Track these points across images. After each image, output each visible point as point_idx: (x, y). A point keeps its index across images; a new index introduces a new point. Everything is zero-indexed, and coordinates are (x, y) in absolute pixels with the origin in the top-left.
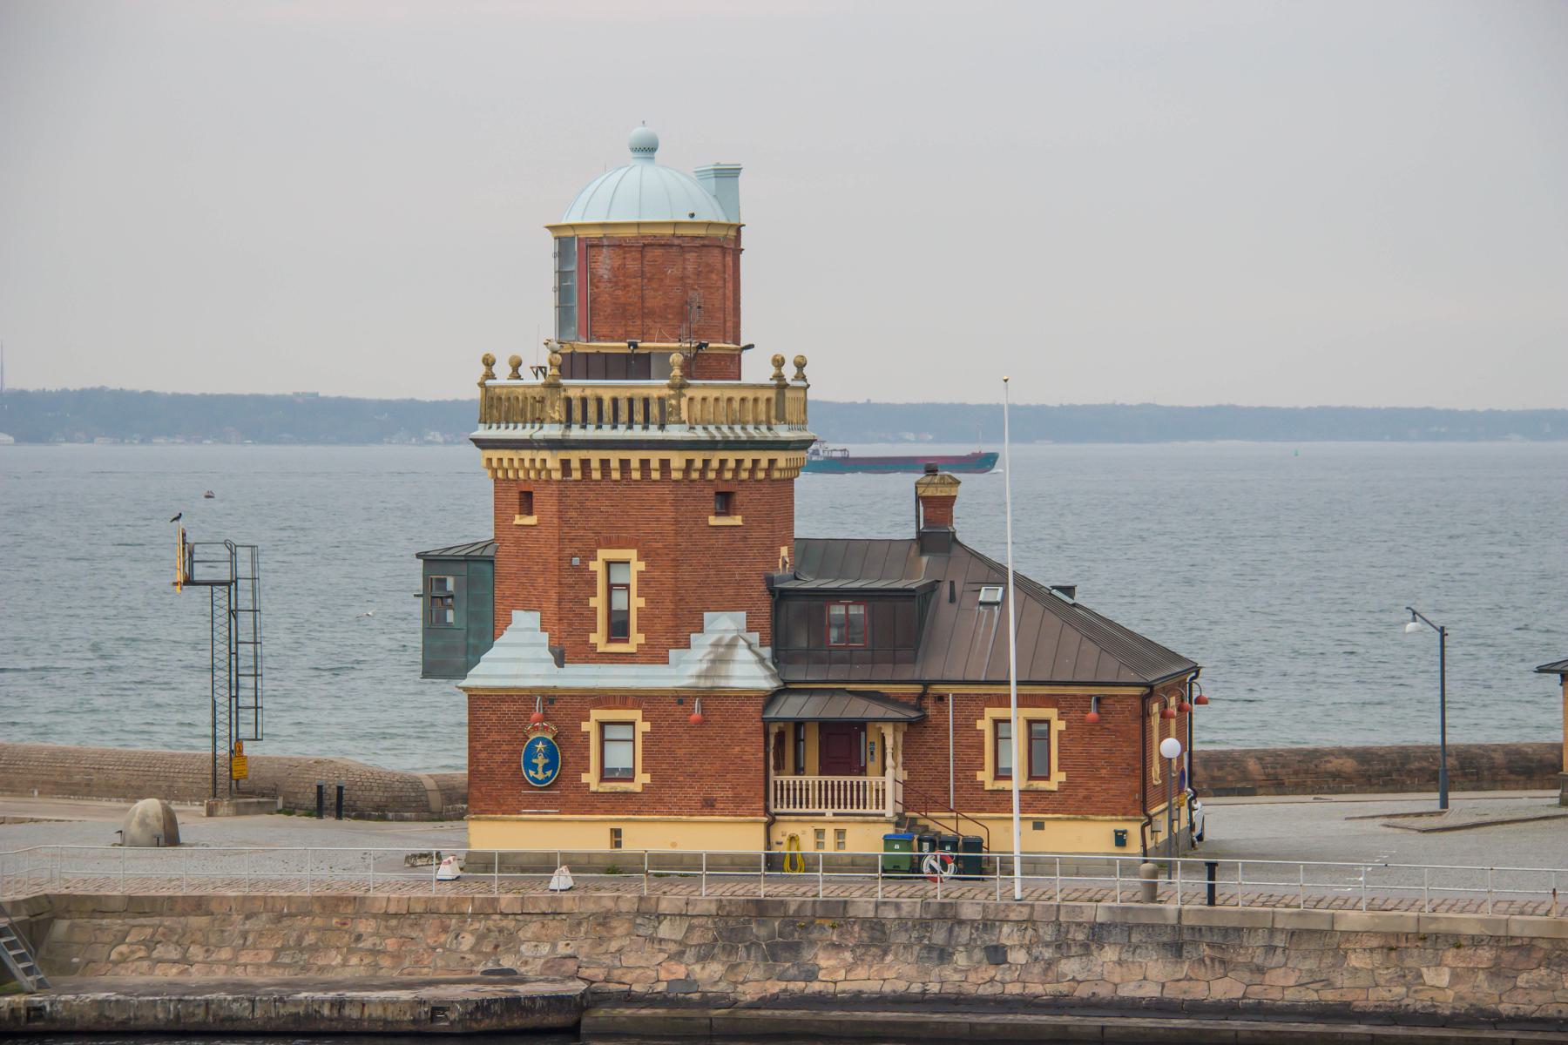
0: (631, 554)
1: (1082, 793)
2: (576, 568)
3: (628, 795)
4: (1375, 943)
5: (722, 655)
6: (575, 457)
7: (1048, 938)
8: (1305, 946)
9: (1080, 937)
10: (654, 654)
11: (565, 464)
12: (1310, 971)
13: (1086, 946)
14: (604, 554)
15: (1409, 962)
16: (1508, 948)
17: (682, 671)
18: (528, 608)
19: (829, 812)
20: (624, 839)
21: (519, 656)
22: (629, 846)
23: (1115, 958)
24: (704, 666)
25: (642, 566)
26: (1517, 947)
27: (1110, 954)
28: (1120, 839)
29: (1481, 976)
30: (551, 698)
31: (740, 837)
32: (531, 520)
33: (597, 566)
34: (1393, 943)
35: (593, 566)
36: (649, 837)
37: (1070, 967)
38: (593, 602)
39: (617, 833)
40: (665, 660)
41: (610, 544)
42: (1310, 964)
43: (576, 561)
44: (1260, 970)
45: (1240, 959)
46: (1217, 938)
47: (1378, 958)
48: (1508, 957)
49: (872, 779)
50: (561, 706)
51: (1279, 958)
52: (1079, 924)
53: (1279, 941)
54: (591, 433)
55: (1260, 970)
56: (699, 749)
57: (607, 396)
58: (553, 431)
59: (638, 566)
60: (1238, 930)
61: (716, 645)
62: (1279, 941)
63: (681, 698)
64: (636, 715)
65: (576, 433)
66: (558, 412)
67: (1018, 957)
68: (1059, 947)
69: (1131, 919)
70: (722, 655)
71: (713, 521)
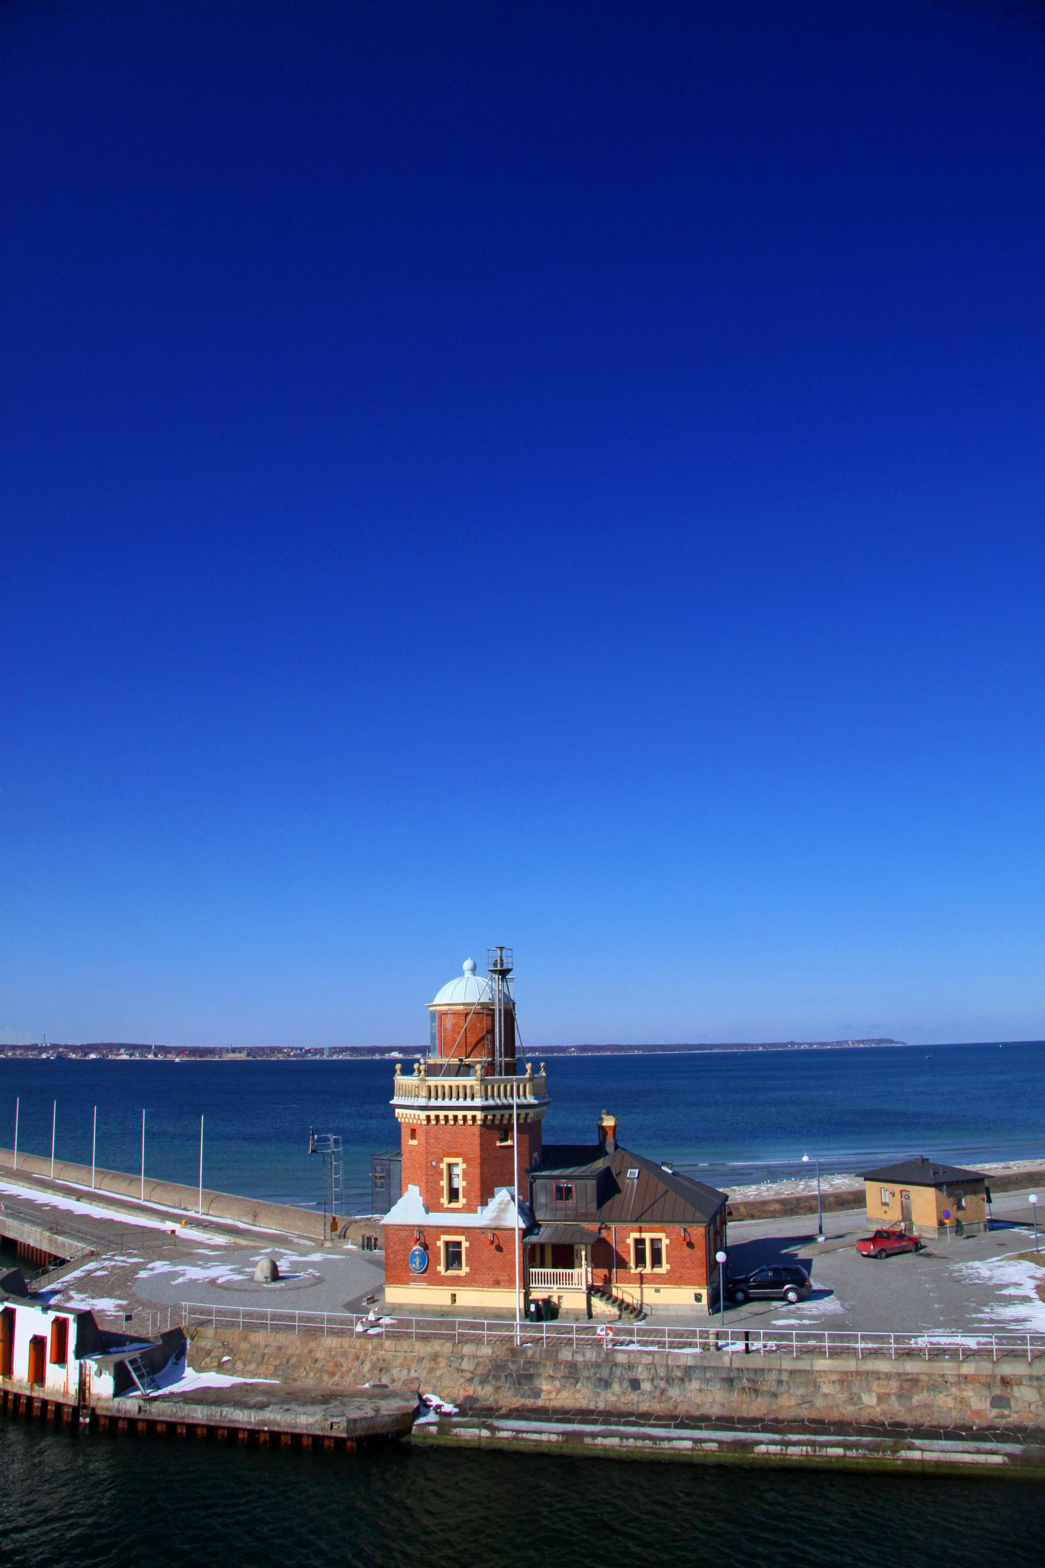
0: (459, 1160)
1: (678, 1275)
2: (435, 1167)
3: (458, 1277)
4: (835, 1377)
5: (502, 1210)
6: (432, 1114)
7: (662, 1375)
8: (798, 1380)
9: (679, 1374)
10: (469, 1209)
11: (428, 1118)
12: (802, 1396)
13: (682, 1380)
14: (448, 1160)
15: (855, 1390)
16: (906, 1380)
17: (482, 1218)
19: (555, 1286)
20: (457, 1298)
22: (459, 1302)
23: (698, 1387)
24: (495, 1214)
25: (464, 1166)
26: (910, 1380)
27: (695, 1385)
28: (698, 1298)
29: (893, 1398)
30: (421, 1229)
32: (415, 1142)
34: (844, 1377)
37: (674, 1392)
39: (454, 1296)
40: (475, 1212)
41: (449, 1155)
42: (801, 1391)
44: (775, 1395)
45: (765, 1388)
46: (751, 1375)
47: (837, 1386)
48: (906, 1385)
49: (575, 1271)
51: (785, 1387)
52: (678, 1367)
53: (785, 1377)
54: (440, 1102)
55: (775, 1395)
58: (422, 1102)
60: (763, 1370)
61: (501, 1203)
62: (785, 1377)
63: (482, 1229)
65: (433, 1102)
66: (424, 1092)
67: (646, 1386)
68: (668, 1381)
69: (706, 1364)
70: (502, 1210)
71: (498, 1144)
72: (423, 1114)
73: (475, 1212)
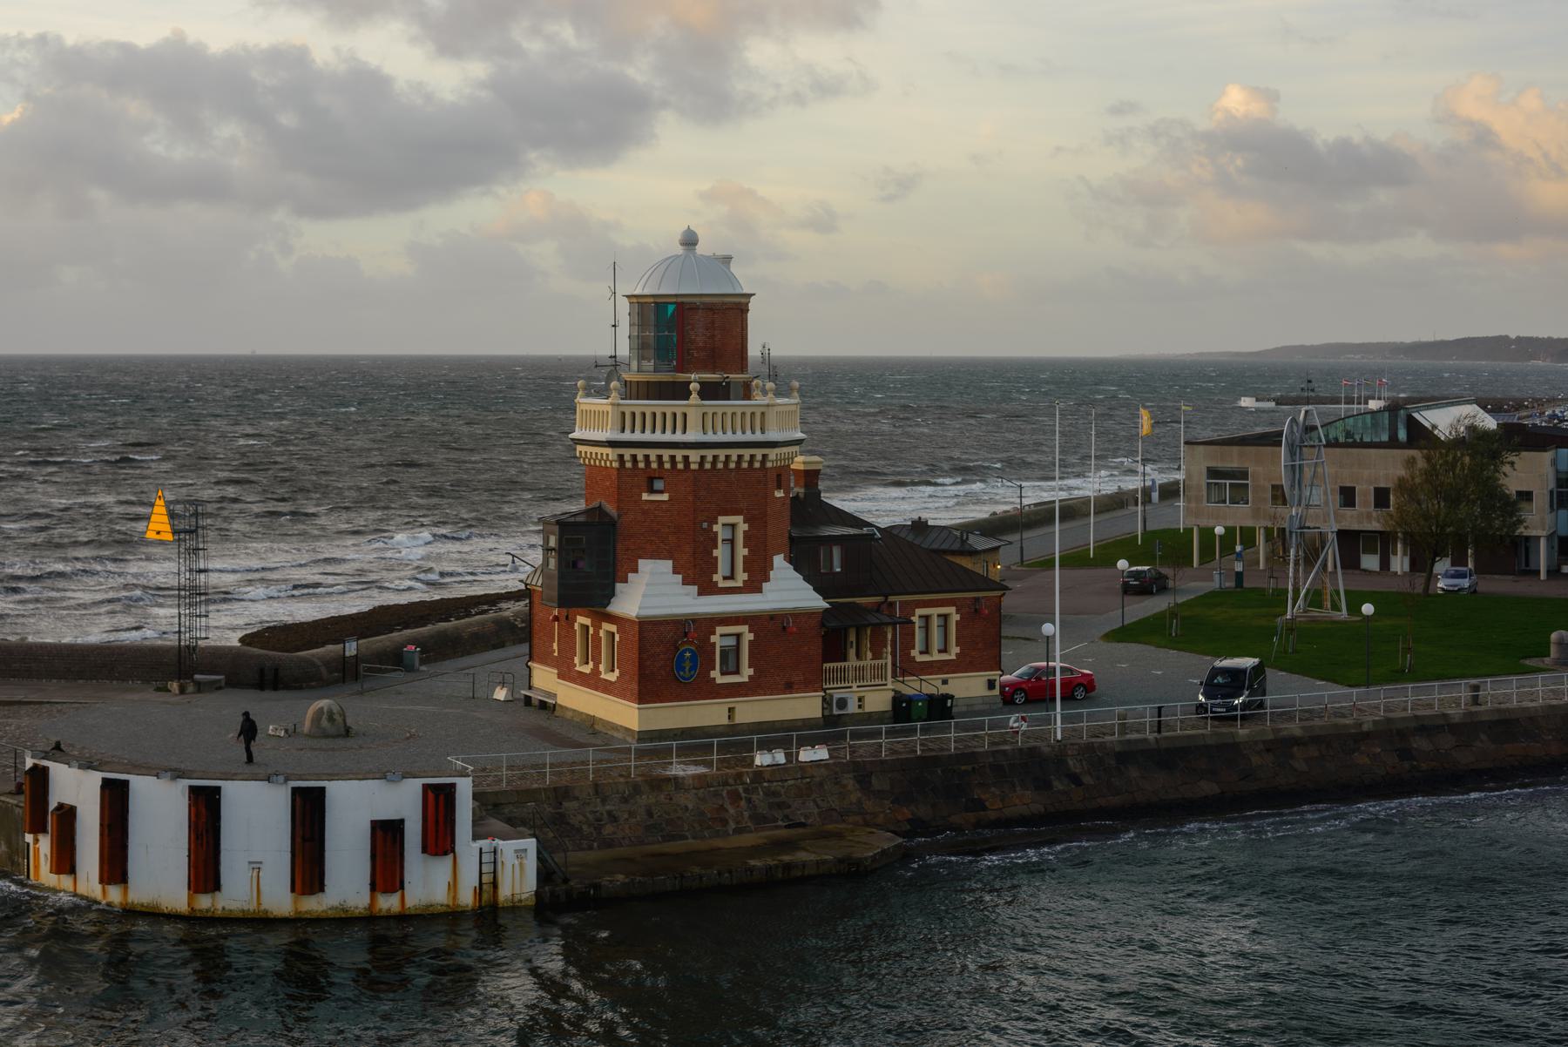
10: (753, 586)
14: (722, 519)
18: (655, 555)
21: (651, 591)
31: (806, 706)
33: (716, 528)
35: (716, 528)
36: (752, 711)
38: (716, 553)
40: (759, 590)
41: (726, 513)
43: (705, 525)
50: (710, 623)
56: (786, 651)
57: (729, 411)
58: (693, 436)
59: (743, 527)
64: (744, 629)
65: (710, 437)
72: (694, 456)
73: (759, 590)
